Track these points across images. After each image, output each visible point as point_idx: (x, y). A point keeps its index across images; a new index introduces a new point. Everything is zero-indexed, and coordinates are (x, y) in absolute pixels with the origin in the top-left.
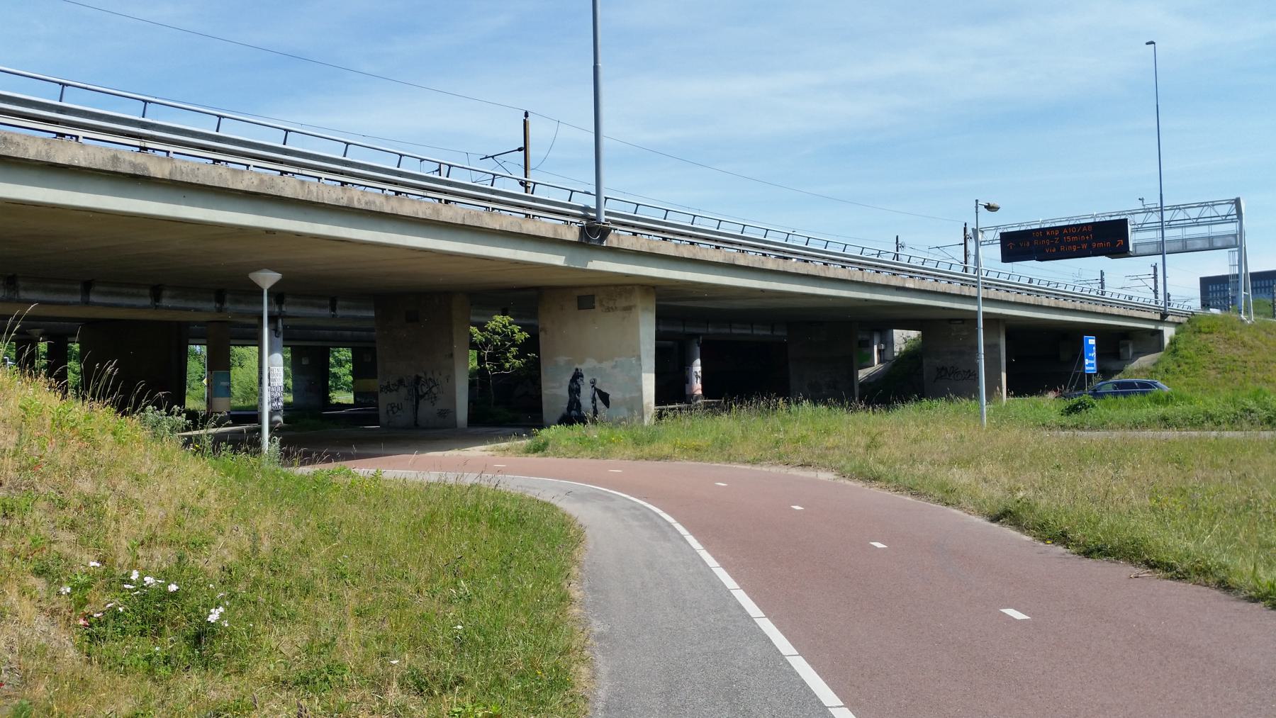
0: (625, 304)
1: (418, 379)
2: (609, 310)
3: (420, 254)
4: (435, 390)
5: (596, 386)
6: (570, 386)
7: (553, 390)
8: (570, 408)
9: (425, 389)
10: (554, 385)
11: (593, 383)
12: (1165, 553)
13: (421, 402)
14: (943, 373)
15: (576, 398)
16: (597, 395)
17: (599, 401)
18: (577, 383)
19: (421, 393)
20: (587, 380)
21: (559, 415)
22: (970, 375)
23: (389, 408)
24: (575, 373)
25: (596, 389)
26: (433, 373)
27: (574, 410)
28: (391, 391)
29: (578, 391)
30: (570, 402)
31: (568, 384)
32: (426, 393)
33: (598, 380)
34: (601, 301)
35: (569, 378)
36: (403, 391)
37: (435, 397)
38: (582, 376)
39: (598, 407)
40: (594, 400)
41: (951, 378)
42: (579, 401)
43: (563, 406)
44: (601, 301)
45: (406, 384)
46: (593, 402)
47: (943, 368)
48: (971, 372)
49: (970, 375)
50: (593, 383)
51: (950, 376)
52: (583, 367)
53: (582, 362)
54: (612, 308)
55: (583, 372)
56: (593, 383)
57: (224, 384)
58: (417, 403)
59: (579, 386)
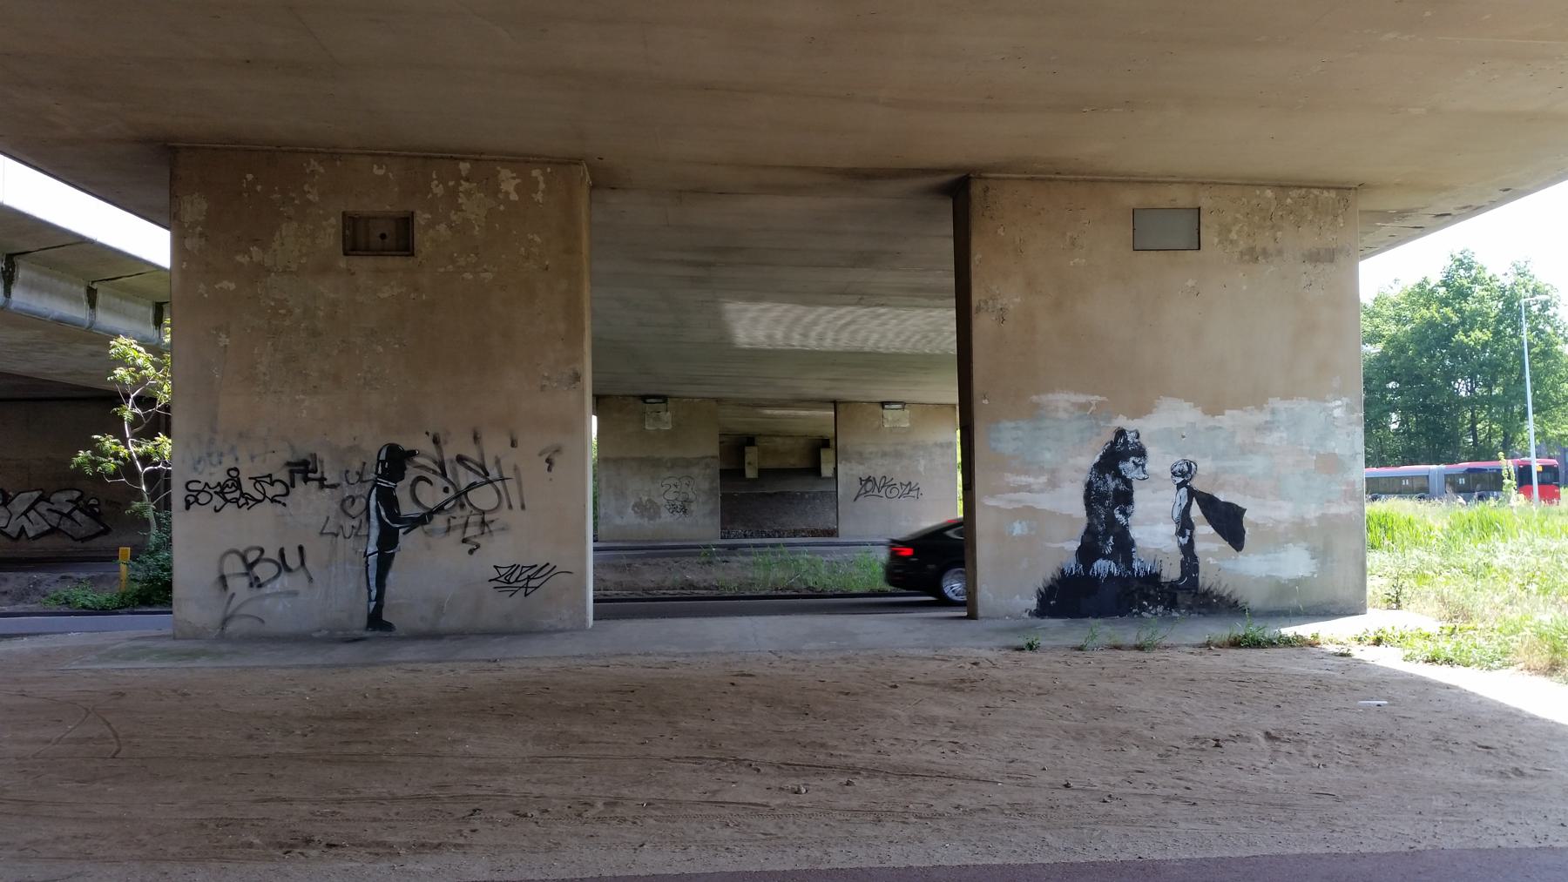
0: (1310, 239)
1: (396, 461)
2: (1253, 255)
3: (39, 166)
4: (483, 498)
5: (1196, 484)
6: (1089, 485)
7: (1023, 495)
8: (1087, 552)
9: (431, 495)
10: (1024, 480)
11: (1184, 476)
12: (1173, 703)
13: (409, 542)
14: (869, 485)
15: (1115, 521)
16: (1196, 511)
17: (1204, 530)
18: (1118, 474)
19: (407, 509)
20: (1160, 462)
21: (1044, 573)
22: (910, 490)
23: (234, 566)
24: (1114, 444)
25: (1192, 493)
26: (476, 438)
27: (1105, 557)
28: (248, 501)
29: (1125, 498)
30: (1090, 532)
31: (1084, 477)
32: (440, 509)
33: (1204, 466)
34: (1224, 231)
35: (1088, 459)
36: (311, 504)
37: (483, 523)
38: (1141, 453)
39: (1199, 547)
40: (1185, 525)
41: (881, 494)
42: (1124, 530)
43: (1064, 548)
44: (1224, 231)
45: (331, 478)
46: (1181, 533)
47: (868, 480)
48: (913, 486)
49: (910, 490)
50: (1183, 474)
51: (879, 492)
52: (1146, 428)
53: (1141, 411)
54: (1265, 252)
55: (1143, 440)
56: (1184, 476)
57: (188, 244)
58: (388, 540)
59: (1128, 483)
